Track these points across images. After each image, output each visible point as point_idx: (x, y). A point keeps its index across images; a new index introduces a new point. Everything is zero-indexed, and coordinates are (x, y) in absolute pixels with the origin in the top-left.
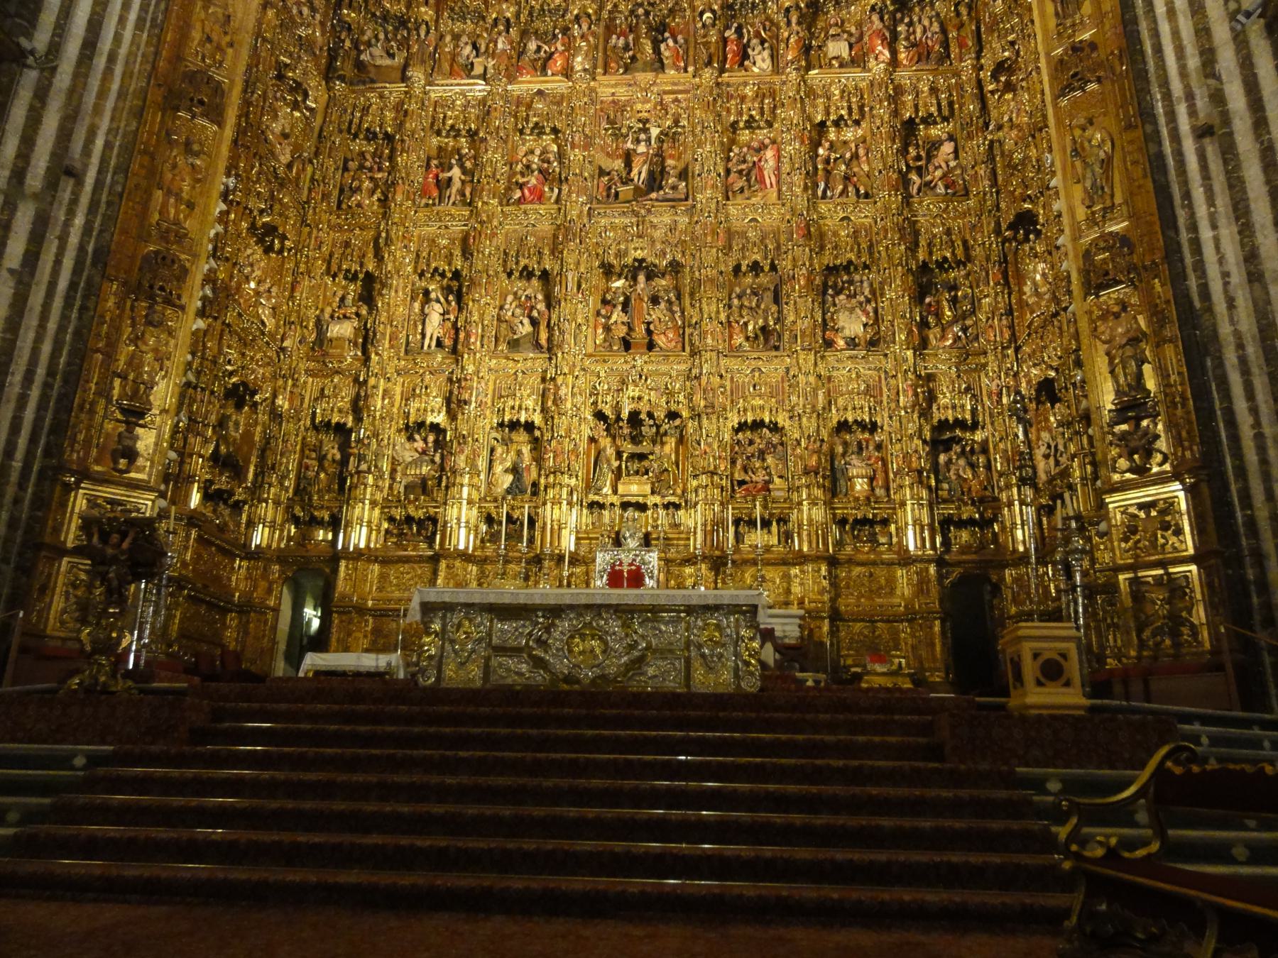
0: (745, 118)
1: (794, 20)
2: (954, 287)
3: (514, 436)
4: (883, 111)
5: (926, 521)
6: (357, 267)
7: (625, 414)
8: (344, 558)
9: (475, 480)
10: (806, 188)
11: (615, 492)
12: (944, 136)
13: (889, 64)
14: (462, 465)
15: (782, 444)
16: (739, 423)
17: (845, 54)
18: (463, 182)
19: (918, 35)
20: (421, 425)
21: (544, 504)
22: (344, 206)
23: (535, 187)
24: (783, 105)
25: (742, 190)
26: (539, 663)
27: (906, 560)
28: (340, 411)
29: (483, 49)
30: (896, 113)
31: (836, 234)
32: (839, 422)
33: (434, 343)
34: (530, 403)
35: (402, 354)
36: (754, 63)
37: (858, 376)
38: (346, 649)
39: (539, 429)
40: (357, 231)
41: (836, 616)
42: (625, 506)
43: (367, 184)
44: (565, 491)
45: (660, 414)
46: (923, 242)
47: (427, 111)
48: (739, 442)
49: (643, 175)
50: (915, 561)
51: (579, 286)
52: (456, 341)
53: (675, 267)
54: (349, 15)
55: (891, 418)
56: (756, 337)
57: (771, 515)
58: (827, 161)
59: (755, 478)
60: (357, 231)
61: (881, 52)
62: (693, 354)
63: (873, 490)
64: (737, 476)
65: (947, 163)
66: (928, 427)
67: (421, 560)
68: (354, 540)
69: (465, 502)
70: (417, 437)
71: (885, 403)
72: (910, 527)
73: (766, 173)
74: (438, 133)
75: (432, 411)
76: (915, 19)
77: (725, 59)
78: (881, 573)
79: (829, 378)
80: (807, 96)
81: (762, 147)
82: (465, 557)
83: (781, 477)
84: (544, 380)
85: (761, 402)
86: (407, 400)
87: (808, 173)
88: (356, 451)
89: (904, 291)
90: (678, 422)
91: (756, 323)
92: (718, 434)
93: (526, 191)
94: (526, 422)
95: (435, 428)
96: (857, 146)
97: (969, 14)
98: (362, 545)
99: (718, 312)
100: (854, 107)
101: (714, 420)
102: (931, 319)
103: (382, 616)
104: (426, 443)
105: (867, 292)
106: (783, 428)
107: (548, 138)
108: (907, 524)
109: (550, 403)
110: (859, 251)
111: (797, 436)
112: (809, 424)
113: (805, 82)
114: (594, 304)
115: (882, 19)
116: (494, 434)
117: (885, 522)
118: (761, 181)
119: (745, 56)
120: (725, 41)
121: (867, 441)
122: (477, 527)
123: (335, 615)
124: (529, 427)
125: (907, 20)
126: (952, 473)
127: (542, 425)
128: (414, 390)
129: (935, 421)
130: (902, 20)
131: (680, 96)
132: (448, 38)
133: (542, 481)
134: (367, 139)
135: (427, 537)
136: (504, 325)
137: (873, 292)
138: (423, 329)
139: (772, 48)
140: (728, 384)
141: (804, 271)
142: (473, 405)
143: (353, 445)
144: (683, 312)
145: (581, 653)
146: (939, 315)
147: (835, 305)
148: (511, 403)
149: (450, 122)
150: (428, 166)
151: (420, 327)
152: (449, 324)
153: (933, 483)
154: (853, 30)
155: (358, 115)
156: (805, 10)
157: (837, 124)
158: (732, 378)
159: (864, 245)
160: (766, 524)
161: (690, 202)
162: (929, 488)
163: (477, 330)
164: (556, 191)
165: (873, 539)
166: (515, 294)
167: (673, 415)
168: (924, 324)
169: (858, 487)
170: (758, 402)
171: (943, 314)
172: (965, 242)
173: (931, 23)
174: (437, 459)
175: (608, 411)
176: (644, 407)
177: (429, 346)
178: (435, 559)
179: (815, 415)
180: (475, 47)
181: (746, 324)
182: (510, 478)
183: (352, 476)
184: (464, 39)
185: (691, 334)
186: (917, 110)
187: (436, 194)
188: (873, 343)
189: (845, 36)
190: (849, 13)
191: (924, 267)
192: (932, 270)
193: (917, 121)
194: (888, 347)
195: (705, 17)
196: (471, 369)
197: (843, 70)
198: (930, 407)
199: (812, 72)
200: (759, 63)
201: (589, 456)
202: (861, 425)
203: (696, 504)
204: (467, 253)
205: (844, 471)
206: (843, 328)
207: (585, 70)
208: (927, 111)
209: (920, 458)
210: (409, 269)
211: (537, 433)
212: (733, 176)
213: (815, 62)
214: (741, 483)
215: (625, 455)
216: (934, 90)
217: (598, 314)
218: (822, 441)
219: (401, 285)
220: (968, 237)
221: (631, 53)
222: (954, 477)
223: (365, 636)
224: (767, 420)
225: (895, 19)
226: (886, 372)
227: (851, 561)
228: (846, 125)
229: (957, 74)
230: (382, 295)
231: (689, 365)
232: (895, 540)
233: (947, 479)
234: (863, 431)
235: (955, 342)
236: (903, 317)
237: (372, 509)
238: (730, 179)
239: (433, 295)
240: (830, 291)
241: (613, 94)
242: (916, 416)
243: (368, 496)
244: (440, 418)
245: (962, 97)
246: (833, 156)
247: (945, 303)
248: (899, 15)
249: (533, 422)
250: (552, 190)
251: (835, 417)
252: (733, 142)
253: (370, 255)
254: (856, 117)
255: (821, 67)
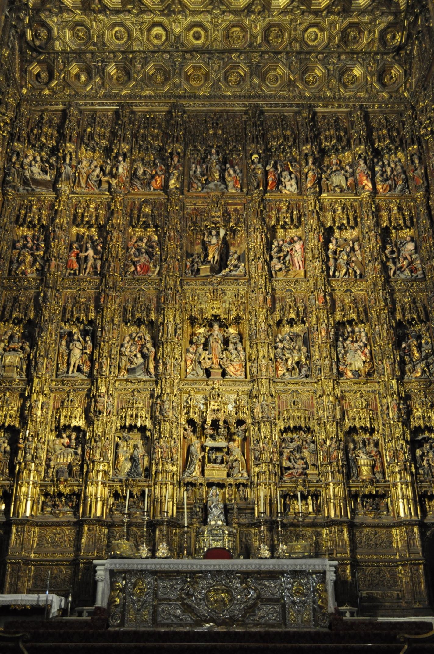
0: (281, 223)
1: (311, 161)
2: (419, 337)
3: (131, 435)
4: (369, 222)
5: (410, 495)
6: (21, 316)
7: (209, 422)
8: (15, 523)
9: (106, 468)
10: (323, 271)
11: (203, 473)
12: (408, 239)
13: (371, 193)
14: (98, 456)
15: (313, 442)
16: (285, 428)
17: (344, 185)
18: (95, 259)
19: (389, 173)
20: (67, 427)
21: (155, 484)
22: (13, 273)
23: (144, 263)
24: (305, 215)
25: (281, 269)
26: (187, 608)
27: (400, 524)
28: (11, 417)
29: (107, 171)
30: (378, 224)
31: (342, 301)
32: (350, 427)
33: (76, 370)
34: (143, 413)
35: (54, 377)
36: (285, 187)
37: (362, 397)
38: (16, 591)
39: (149, 430)
40: (22, 291)
41: (355, 564)
42: (210, 485)
43: (29, 259)
44: (169, 475)
45: (233, 422)
46: (398, 308)
47: (70, 211)
48: (284, 440)
49: (216, 258)
50: (404, 524)
51: (176, 333)
52: (92, 368)
53: (238, 320)
54: (18, 146)
55: (384, 425)
56: (294, 369)
57: (309, 491)
58: (335, 252)
59: (296, 466)
60: (22, 291)
61: (366, 184)
62: (252, 381)
63: (374, 473)
64: (286, 464)
65: (411, 256)
66: (408, 432)
67: (68, 524)
68: (22, 509)
69: (100, 483)
70: (64, 435)
71: (379, 414)
72: (401, 500)
73: (296, 259)
74: (78, 226)
75: (76, 418)
76: (386, 163)
77: (267, 184)
78: (382, 532)
79: (343, 397)
80: (321, 209)
81: (292, 241)
82: (99, 521)
83: (313, 465)
84: (152, 396)
85: (299, 414)
86: (58, 409)
87: (323, 261)
88: (23, 446)
89: (388, 340)
90: (243, 427)
91: (293, 359)
92: (271, 436)
93: (138, 268)
94: (141, 425)
95: (77, 429)
96: (353, 243)
97: (419, 163)
98: (28, 514)
99: (268, 352)
100: (351, 218)
101: (268, 426)
102: (407, 358)
103: (41, 565)
104: (70, 439)
105: (364, 340)
106: (314, 431)
107: (150, 231)
108: (398, 498)
109: (157, 414)
110: (358, 313)
111: (324, 437)
112: (332, 429)
113: (319, 200)
114: (185, 345)
115: (365, 163)
116: (118, 434)
117: (384, 496)
118: (293, 265)
119: (279, 182)
120: (266, 173)
121: (369, 440)
122: (108, 500)
123: (8, 565)
124: (143, 429)
125: (380, 163)
126: (425, 462)
127: (152, 428)
128: (63, 403)
129: (412, 427)
130: (378, 163)
131: (238, 207)
132: (84, 163)
133: (154, 468)
134: (28, 227)
135: (72, 507)
136: (124, 358)
137: (368, 339)
138: (69, 359)
139: (296, 178)
140: (276, 400)
141: (324, 325)
142: (105, 414)
143: (21, 441)
144: (244, 349)
145: (216, 601)
146: (411, 356)
147: (344, 348)
148: (130, 412)
149: (86, 219)
150: (71, 248)
151: (66, 358)
152: (86, 357)
153: (413, 470)
154: (348, 168)
155: (23, 212)
156: (317, 156)
157: (340, 228)
158: (279, 396)
159: (361, 309)
160: (304, 497)
161: (247, 277)
162: (411, 473)
163: (106, 362)
164: (158, 268)
165: (377, 508)
166: (131, 335)
167: (240, 422)
168: (402, 363)
169: (365, 473)
170: (297, 413)
171: (413, 355)
172: (425, 308)
173: (396, 166)
174: (79, 451)
175: (196, 418)
176: (221, 416)
177: (73, 372)
178: (79, 525)
179: (335, 423)
180: (102, 169)
181: (287, 360)
182: (129, 465)
183: (20, 464)
184: (95, 163)
185: (251, 366)
186: (390, 222)
187: (76, 266)
188: (369, 374)
189: (343, 172)
190: (344, 156)
191: (400, 324)
192: (405, 326)
193: (391, 228)
194: (380, 378)
195: (253, 157)
196: (103, 390)
197: (343, 194)
198: (409, 417)
199: (324, 195)
200: (288, 187)
201: (184, 449)
202: (365, 430)
203: (258, 485)
204: (99, 309)
205: (355, 461)
206: (351, 364)
207: (176, 188)
208: (397, 223)
209: (404, 453)
210: (59, 318)
211: (148, 433)
212: (275, 261)
213: (324, 188)
214: (288, 468)
215: (207, 449)
216: (400, 209)
217: (187, 351)
218: (341, 440)
219: (54, 330)
220: (426, 305)
221: (205, 177)
222: (426, 466)
223: (29, 581)
224: (303, 426)
225: (373, 162)
226: (379, 393)
227: (363, 525)
228: (346, 229)
229: (414, 200)
230: (42, 337)
231: (250, 388)
232: (390, 508)
233: (422, 466)
234: (365, 434)
235: (422, 374)
236: (389, 358)
237: (35, 487)
238: (272, 264)
239: (76, 337)
240: (341, 339)
241: (195, 204)
242: (400, 424)
243: (32, 478)
244: (80, 422)
245: (418, 214)
246: (339, 249)
247: (414, 348)
248: (376, 160)
249: (145, 426)
250: (155, 266)
251: (348, 424)
252: (274, 237)
253: (32, 308)
254: (352, 223)
255: (328, 192)
